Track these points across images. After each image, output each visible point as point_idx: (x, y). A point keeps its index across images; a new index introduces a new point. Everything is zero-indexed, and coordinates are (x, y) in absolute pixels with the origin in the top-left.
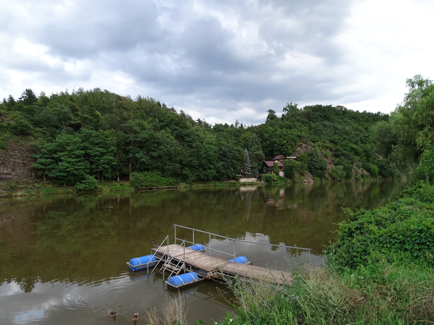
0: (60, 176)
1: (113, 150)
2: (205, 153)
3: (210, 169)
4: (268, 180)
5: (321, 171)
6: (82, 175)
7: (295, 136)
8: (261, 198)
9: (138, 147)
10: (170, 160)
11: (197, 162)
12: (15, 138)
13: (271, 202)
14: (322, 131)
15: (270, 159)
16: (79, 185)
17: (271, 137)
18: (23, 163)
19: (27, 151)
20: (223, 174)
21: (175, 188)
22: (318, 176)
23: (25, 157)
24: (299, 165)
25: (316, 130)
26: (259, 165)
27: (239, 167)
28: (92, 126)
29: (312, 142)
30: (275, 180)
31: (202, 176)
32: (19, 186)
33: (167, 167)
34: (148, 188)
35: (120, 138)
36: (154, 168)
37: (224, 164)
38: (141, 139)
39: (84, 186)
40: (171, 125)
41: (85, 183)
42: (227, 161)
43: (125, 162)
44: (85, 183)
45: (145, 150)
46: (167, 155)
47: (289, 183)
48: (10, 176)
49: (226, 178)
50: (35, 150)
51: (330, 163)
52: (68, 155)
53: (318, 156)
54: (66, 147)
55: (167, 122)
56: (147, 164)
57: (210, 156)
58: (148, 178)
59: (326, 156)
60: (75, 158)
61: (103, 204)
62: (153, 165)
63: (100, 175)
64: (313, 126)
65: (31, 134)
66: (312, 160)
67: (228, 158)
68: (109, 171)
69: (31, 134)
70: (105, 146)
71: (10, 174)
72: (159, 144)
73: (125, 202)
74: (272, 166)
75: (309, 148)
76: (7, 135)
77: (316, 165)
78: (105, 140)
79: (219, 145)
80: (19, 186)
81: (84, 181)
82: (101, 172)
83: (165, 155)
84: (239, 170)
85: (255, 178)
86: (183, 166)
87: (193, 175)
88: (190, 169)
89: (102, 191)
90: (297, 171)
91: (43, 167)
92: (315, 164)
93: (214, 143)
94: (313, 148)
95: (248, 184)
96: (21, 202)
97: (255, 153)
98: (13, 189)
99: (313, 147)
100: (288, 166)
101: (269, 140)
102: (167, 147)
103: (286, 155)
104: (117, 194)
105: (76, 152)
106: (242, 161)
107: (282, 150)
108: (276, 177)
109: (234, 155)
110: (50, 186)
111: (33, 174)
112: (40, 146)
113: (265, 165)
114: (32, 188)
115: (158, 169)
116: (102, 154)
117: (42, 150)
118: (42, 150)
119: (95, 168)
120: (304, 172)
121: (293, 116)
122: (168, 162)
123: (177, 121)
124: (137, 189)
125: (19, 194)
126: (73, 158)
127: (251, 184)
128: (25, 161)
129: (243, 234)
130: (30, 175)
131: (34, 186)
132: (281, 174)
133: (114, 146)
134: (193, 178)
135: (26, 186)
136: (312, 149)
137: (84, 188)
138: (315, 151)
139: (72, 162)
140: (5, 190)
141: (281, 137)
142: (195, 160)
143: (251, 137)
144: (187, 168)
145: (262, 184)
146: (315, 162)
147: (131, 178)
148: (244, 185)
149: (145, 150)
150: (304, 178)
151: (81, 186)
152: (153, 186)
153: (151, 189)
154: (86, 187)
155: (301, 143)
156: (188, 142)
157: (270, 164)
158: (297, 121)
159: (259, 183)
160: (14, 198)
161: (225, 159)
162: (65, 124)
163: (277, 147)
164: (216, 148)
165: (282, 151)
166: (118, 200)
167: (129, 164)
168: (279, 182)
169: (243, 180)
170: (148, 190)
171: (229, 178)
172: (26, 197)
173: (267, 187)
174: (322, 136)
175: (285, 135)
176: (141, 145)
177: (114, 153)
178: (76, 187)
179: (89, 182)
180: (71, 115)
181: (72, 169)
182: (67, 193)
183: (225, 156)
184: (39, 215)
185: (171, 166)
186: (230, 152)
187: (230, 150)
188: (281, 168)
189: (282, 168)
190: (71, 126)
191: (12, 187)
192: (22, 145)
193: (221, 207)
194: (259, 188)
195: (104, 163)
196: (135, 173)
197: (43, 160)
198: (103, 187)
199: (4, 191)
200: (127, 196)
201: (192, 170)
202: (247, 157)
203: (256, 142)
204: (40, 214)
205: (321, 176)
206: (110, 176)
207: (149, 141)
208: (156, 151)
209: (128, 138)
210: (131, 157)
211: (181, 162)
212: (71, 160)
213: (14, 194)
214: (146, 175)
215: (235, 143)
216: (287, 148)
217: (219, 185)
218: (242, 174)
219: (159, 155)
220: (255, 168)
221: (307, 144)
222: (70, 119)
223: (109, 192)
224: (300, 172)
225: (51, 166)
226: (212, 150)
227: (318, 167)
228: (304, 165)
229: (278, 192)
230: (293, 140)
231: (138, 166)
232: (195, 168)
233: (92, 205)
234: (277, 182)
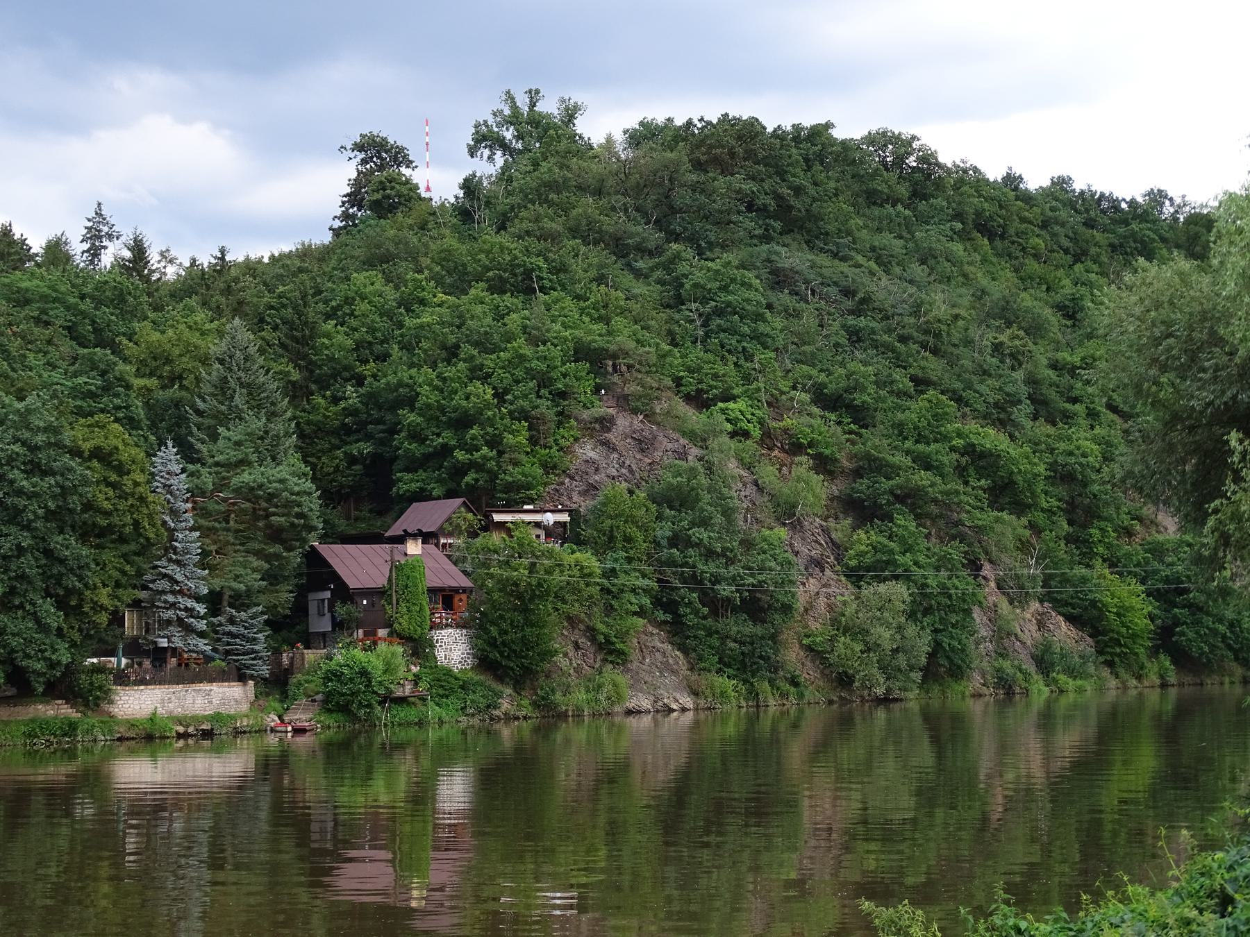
4: (346, 699)
5: (749, 628)
7: (556, 352)
13: (364, 875)
14: (759, 317)
22: (724, 663)
25: (719, 312)
26: (272, 578)
29: (688, 398)
30: (402, 700)
47: (509, 718)
51: (819, 564)
53: (728, 513)
59: (787, 514)
64: (699, 276)
66: (689, 543)
74: (380, 581)
75: (666, 444)
77: (716, 580)
84: (103, 618)
85: (242, 679)
90: (572, 621)
94: (695, 451)
97: (246, 477)
99: (692, 436)
100: (503, 584)
103: (486, 497)
106: (137, 544)
107: (460, 455)
113: (319, 573)
120: (623, 636)
121: (546, 191)
127: (206, 734)
132: (453, 648)
136: (682, 455)
138: (709, 467)
141: (452, 353)
143: (216, 347)
145: (298, 731)
146: (710, 554)
148: (149, 737)
150: (622, 680)
155: (601, 410)
157: (360, 565)
158: (574, 232)
159: (272, 719)
163: (416, 436)
165: (460, 471)
168: (433, 711)
169: (136, 703)
173: (341, 754)
174: (761, 356)
175: (484, 344)
186: (36, 469)
187: (34, 449)
188: (448, 604)
189: (461, 602)
194: (273, 767)
202: (174, 513)
203: (252, 390)
205: (749, 664)
215: (76, 393)
216: (494, 442)
218: (134, 649)
220: (240, 601)
224: (591, 632)
227: (725, 590)
228: (622, 580)
229: (422, 797)
230: (544, 381)
234: (410, 714)
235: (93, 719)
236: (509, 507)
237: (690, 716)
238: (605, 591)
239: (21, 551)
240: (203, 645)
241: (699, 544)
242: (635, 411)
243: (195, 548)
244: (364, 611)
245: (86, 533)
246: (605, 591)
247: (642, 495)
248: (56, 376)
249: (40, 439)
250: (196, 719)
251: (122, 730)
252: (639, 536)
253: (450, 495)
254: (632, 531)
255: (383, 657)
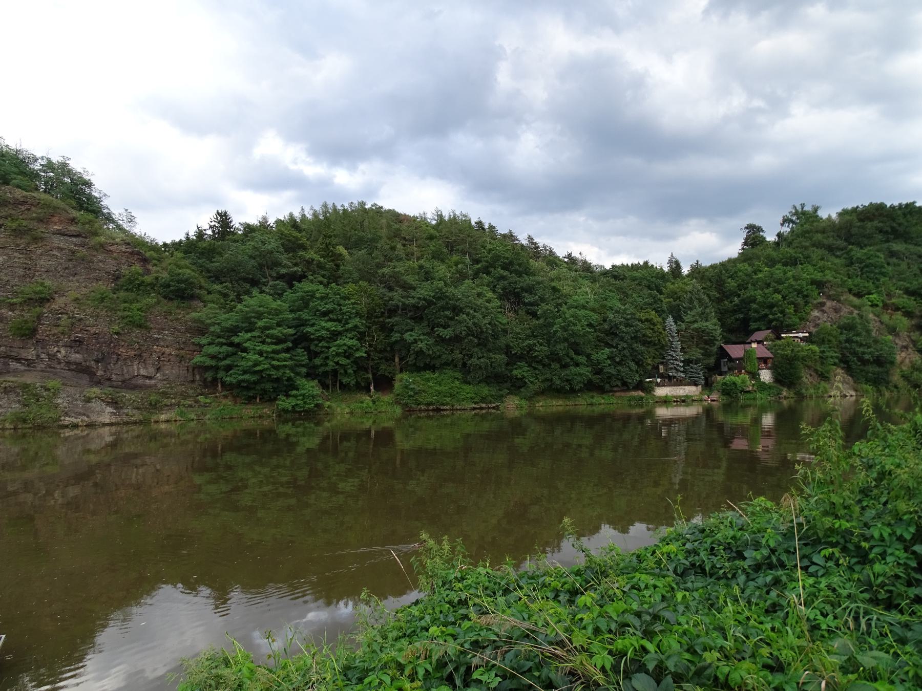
0: (243, 381)
1: (356, 326)
2: (565, 329)
3: (577, 365)
4: (729, 391)
5: (877, 369)
6: (289, 379)
7: (804, 283)
8: (715, 435)
9: (411, 318)
10: (482, 344)
11: (546, 348)
12: (166, 305)
13: (739, 444)
14: (882, 267)
15: (741, 340)
16: (284, 401)
17: (742, 287)
18: (177, 356)
19: (188, 330)
20: (609, 378)
21: (494, 408)
22: (867, 381)
23: (184, 343)
24: (814, 352)
25: (867, 266)
26: (707, 354)
27: (649, 361)
28: (323, 276)
29: (855, 295)
30: (749, 392)
31: (558, 382)
32: (167, 401)
33: (474, 361)
34: (431, 408)
35: (373, 300)
36: (447, 364)
37: (612, 352)
38: (416, 300)
39: (293, 401)
40: (495, 268)
41: (295, 396)
42: (620, 347)
43: (385, 350)
44: (295, 396)
45: (425, 323)
46: (473, 335)
47: (786, 398)
48: (153, 382)
49: (617, 386)
50: (201, 329)
51: (906, 347)
52: (259, 337)
53: (868, 332)
54: (256, 320)
55: (487, 262)
56: (429, 355)
57: (574, 335)
58: (430, 387)
59: (893, 330)
60: (272, 343)
61: (333, 444)
62: (444, 357)
63: (331, 380)
64: (859, 255)
65: (199, 298)
66: (853, 342)
67: (622, 339)
68: (350, 371)
69: (199, 298)
70: (340, 317)
71: (151, 378)
72: (457, 310)
73: (385, 437)
75: (845, 310)
76: (151, 300)
77: (864, 353)
78: (339, 305)
79: (601, 309)
80: (167, 401)
81: (294, 392)
82: (335, 373)
83: (468, 335)
84: (650, 368)
85: (696, 385)
86: (513, 358)
87: (537, 378)
88: (530, 366)
89: (333, 414)
90: (809, 367)
91: (213, 363)
92: (861, 350)
93: (591, 304)
94: (856, 312)
95: (677, 400)
96: (170, 434)
97: (696, 325)
98: (155, 407)
99: (855, 307)
100: (782, 356)
101: (739, 296)
102: (474, 317)
104: (365, 420)
105: (274, 332)
106: (661, 348)
107: (771, 317)
108: (750, 384)
109: (637, 332)
110: (228, 402)
111: (198, 377)
112: (208, 321)
113: (723, 353)
114: (191, 406)
115: (456, 366)
116: (335, 335)
117: (212, 329)
118: (212, 329)
119: (321, 365)
120: (828, 372)
121: (804, 234)
122: (476, 349)
123: (507, 258)
124: (409, 411)
125: (163, 417)
126: (269, 344)
127: (684, 401)
128: (183, 352)
129: (596, 529)
130: (190, 378)
131: (197, 402)
132: (766, 376)
133: (361, 317)
134: (535, 385)
135: (179, 402)
136: (851, 313)
137: (293, 407)
138: (861, 317)
139: (267, 352)
140: (138, 408)
141: (768, 285)
142: (541, 345)
143: (689, 288)
144: (523, 364)
145: (712, 401)
146: (861, 345)
147: (397, 385)
148: (665, 402)
149: (425, 323)
150: (827, 386)
151: (285, 403)
152: (443, 404)
153: (438, 410)
154: (297, 405)
156: (531, 304)
157: (735, 351)
158: (814, 245)
160: (154, 426)
161: (615, 341)
162: (270, 275)
163: (756, 311)
164: (595, 316)
165: (771, 321)
166: (373, 433)
167: (394, 356)
168: (758, 395)
169: (662, 392)
170: (431, 413)
171: (626, 386)
172: (178, 423)
173: (727, 408)
174: (883, 279)
175: (780, 282)
176: (418, 313)
177: (359, 333)
178: (278, 405)
179: (303, 395)
180: (284, 258)
181: (266, 366)
182: (260, 417)
183: (616, 334)
184: (209, 461)
185: (482, 360)
186: (627, 325)
187: (628, 320)
190: (281, 277)
191: (151, 404)
192: (177, 319)
193: (605, 454)
194: (708, 411)
195: (338, 355)
196: (405, 376)
197: (213, 350)
198: (334, 405)
199: (135, 412)
200: (386, 425)
201: (535, 369)
202: (673, 337)
203: (700, 300)
204: (211, 457)
205: (878, 381)
206: (353, 382)
207: (435, 304)
208: (449, 326)
209: (391, 299)
210: (396, 342)
211: (507, 350)
212: (265, 348)
213: (154, 418)
214: (428, 380)
215: (646, 304)
216: (782, 312)
217: (601, 403)
218: (661, 376)
219: (457, 336)
220: (697, 362)
221: (839, 301)
222: (277, 264)
223: (347, 416)
224: (816, 371)
225: (227, 362)
226: (580, 321)
227: (867, 357)
228: (827, 354)
229: (757, 421)
231: (411, 360)
232: (540, 362)
233: (313, 442)
234: (751, 396)
235: (649, 396)
236: (789, 332)
237: (854, 398)
238: (820, 357)
239: (624, 349)
240: (682, 375)
241: (857, 342)
242: (833, 300)
243: (679, 347)
244: (737, 365)
245: (644, 343)
246: (820, 357)
247: (835, 326)
248: (640, 299)
249: (629, 317)
250: (680, 397)
251: (657, 399)
252: (834, 340)
253: (768, 329)
254: (831, 338)
255: (741, 379)
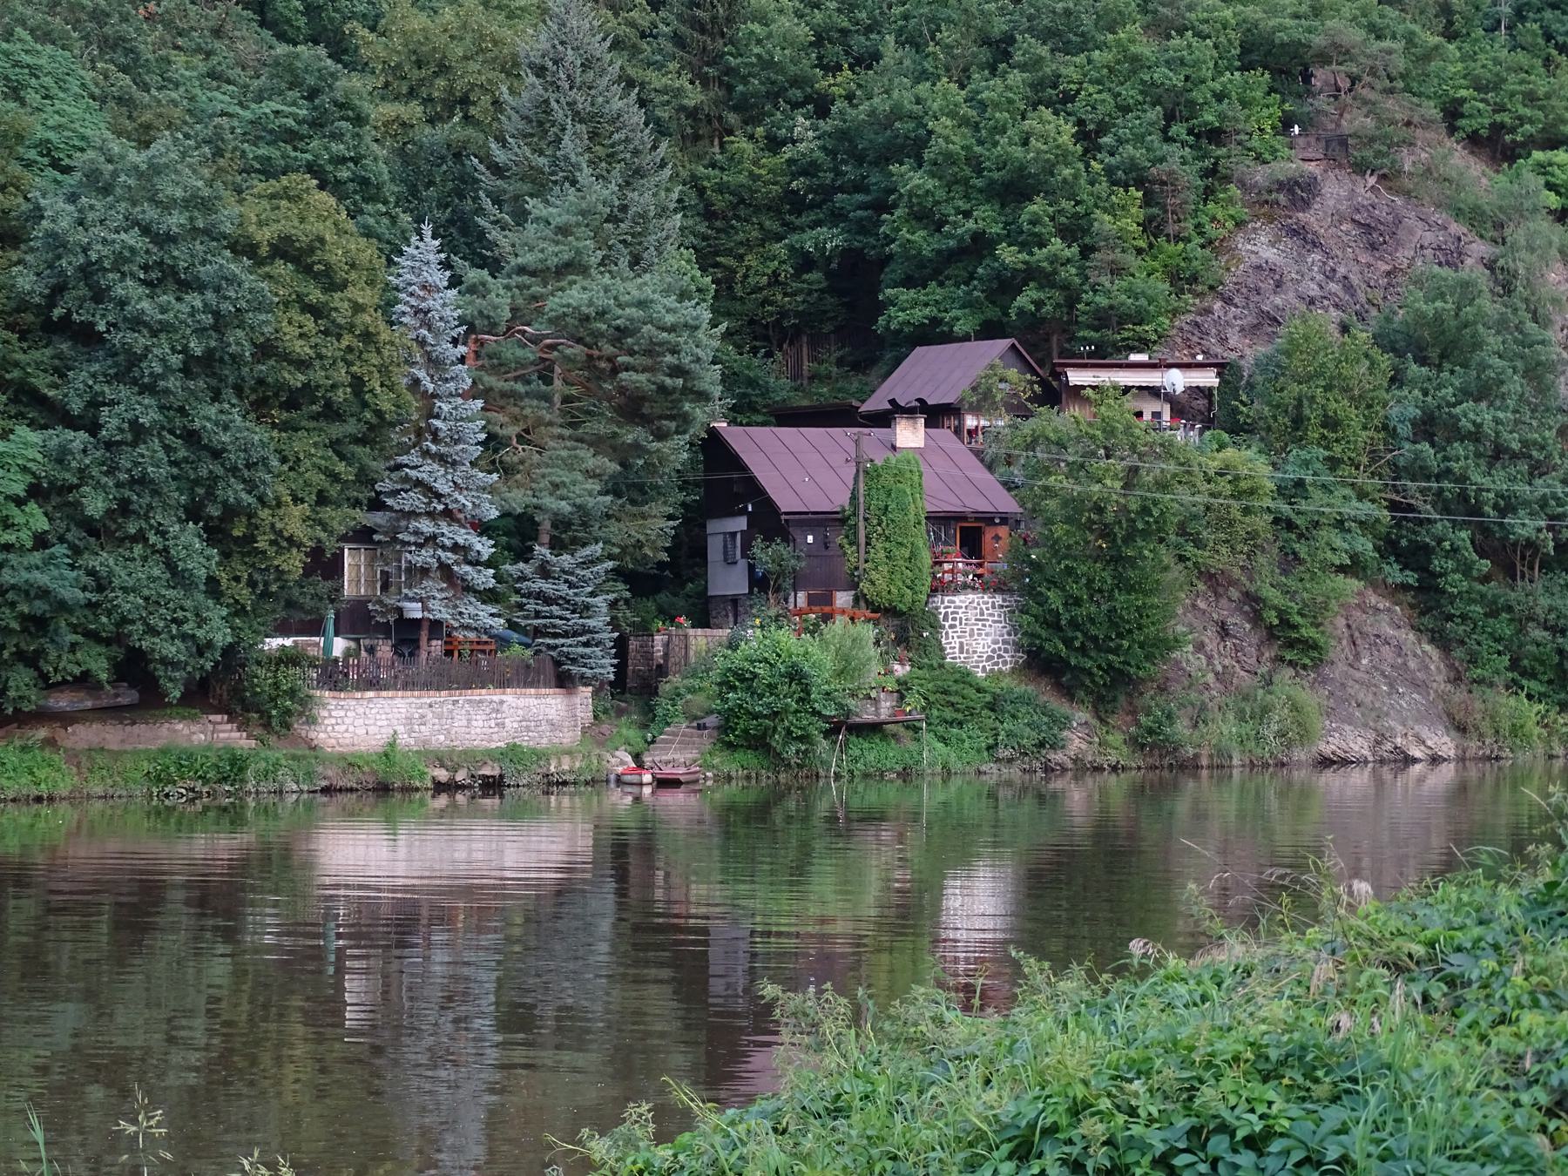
4: (755, 724)
8: (660, 1003)
20: (37, 625)
24: (1245, 493)
26: (630, 488)
27: (294, 521)
29: (1474, 141)
30: (875, 729)
37: (60, 457)
42: (111, 422)
47: (1082, 769)
49: (84, 681)
67: (127, 368)
74: (839, 499)
75: (1422, 232)
77: (1508, 505)
84: (294, 563)
85: (564, 682)
90: (1215, 581)
94: (1479, 249)
97: (575, 295)
99: (1475, 217)
101: (822, 106)
103: (1050, 343)
106: (362, 426)
107: (1008, 255)
109: (220, 323)
113: (723, 482)
120: (1315, 612)
127: (489, 785)
132: (976, 631)
136: (1452, 256)
138: (1505, 284)
141: (1000, 50)
145: (663, 783)
146: (1499, 454)
148: (382, 788)
150: (1310, 698)
155: (1289, 166)
157: (800, 467)
159: (621, 761)
161: (81, 377)
163: (925, 216)
165: (1007, 284)
168: (931, 751)
169: (357, 723)
171: (139, 685)
173: (748, 827)
183: (87, 337)
186: (165, 277)
187: (165, 240)
188: (972, 543)
189: (998, 543)
194: (626, 854)
203: (596, 126)
215: (258, 131)
216: (1075, 230)
218: (357, 620)
224: (1253, 604)
227: (1525, 526)
229: (912, 915)
230: (1176, 108)
235: (278, 751)
236: (1102, 356)
237: (1448, 772)
238: (1283, 523)
239: (138, 432)
240: (486, 616)
241: (1476, 436)
242: (1360, 168)
243: (475, 431)
244: (804, 556)
245: (264, 400)
246: (1283, 523)
247: (1363, 336)
248: (222, 99)
249: (175, 221)
250: (471, 757)
251: (332, 775)
252: (1353, 416)
253: (989, 331)
254: (1340, 406)
255: (835, 649)
